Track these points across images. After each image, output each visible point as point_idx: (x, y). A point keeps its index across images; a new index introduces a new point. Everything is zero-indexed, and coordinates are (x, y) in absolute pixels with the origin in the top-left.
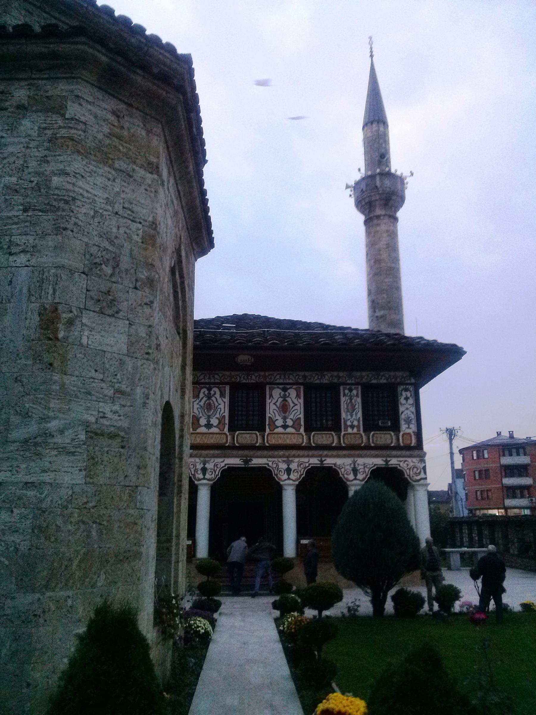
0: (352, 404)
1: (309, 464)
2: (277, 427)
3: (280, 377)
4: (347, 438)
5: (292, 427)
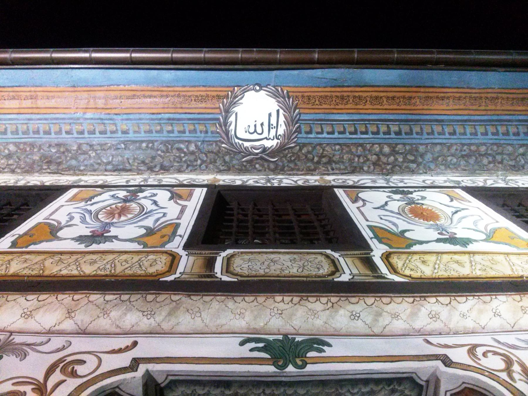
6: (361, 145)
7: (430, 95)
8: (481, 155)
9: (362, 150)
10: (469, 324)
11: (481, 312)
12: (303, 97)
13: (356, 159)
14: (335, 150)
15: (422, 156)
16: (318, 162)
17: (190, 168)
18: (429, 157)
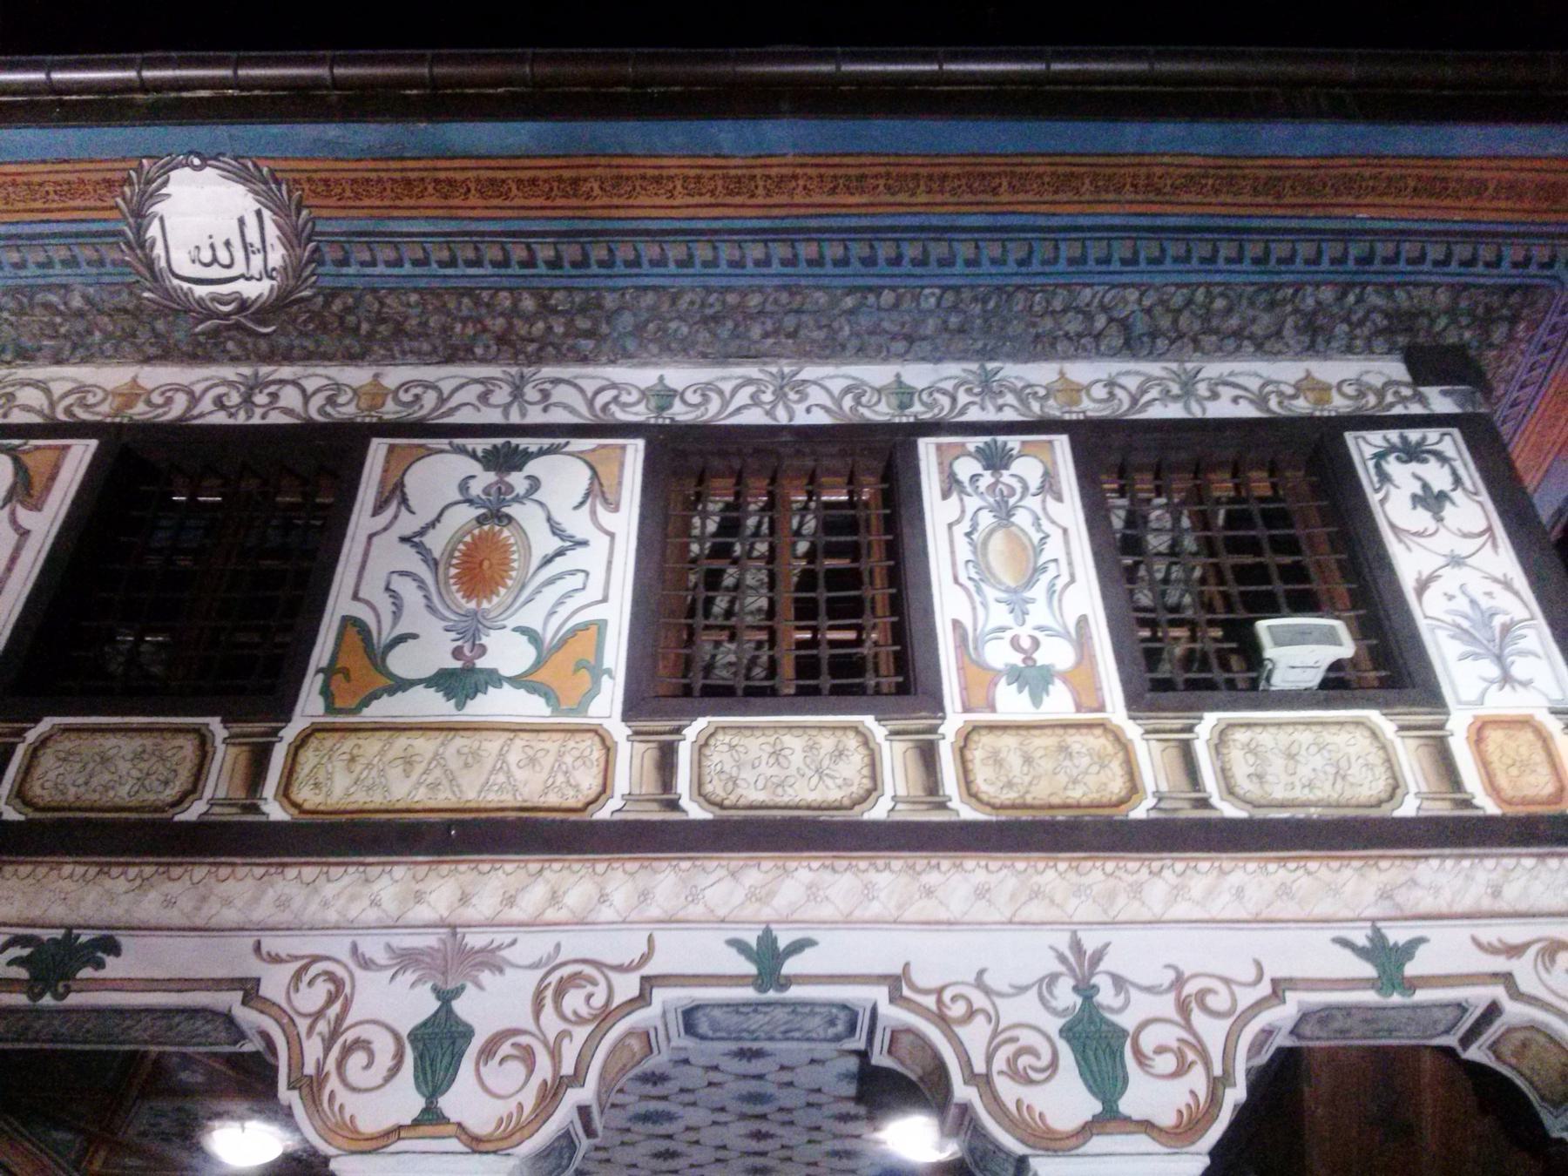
0: (1018, 542)
1: (648, 982)
2: (401, 685)
3: (484, 398)
4: (996, 759)
5: (517, 681)
6: (469, 292)
7: (625, 172)
8: (749, 317)
9: (470, 304)
10: (332, 916)
11: (353, 898)
12: (309, 180)
13: (458, 327)
14: (409, 305)
15: (610, 317)
16: (371, 335)
17: (80, 352)
18: (627, 320)
